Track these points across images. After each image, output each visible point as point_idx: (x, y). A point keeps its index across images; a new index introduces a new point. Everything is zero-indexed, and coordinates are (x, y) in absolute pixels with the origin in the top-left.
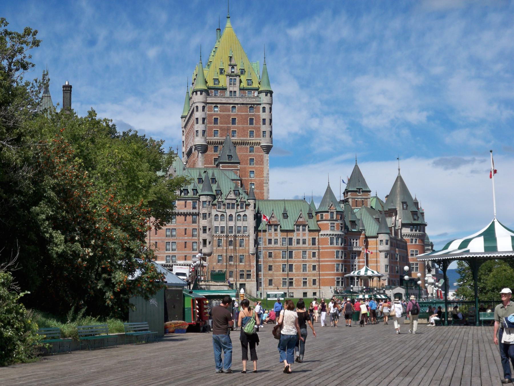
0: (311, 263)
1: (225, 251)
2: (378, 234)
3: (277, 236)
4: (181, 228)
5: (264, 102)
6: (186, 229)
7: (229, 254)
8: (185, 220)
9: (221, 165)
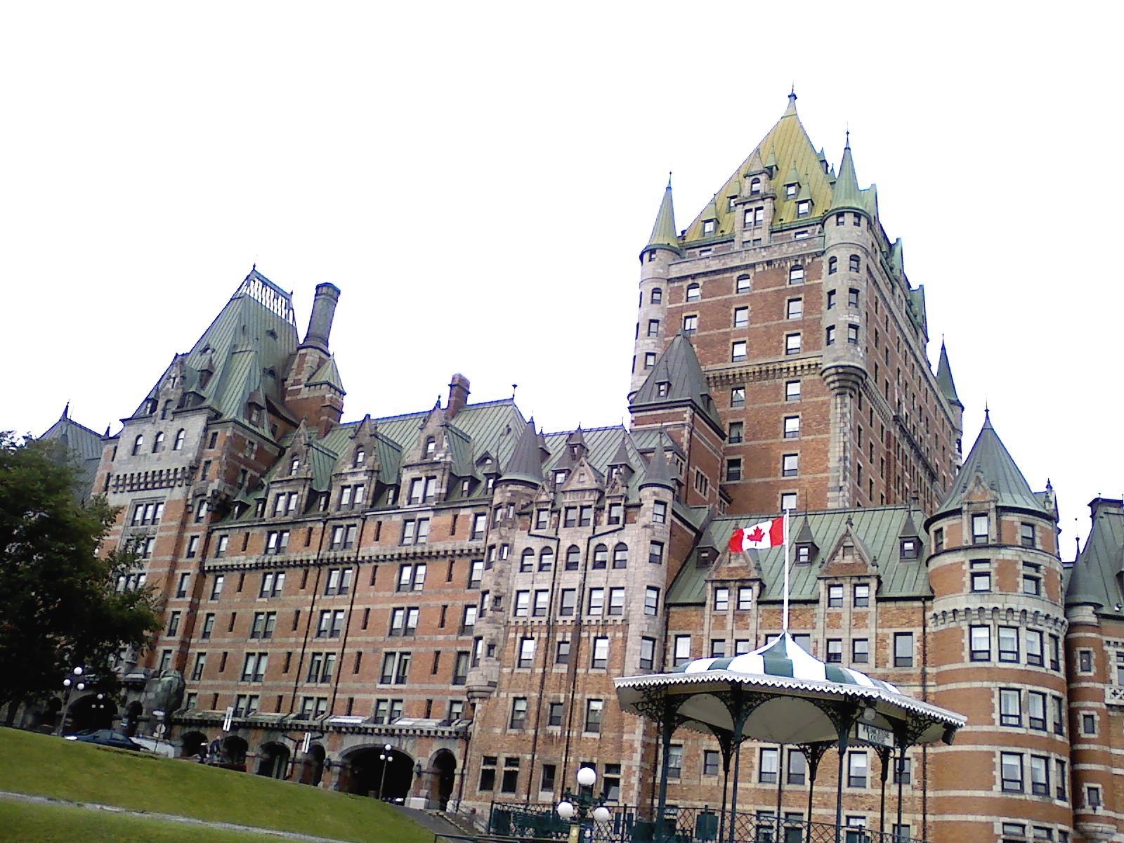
1: (537, 681)
4: (432, 603)
5: (832, 242)
6: (445, 607)
7: (550, 695)
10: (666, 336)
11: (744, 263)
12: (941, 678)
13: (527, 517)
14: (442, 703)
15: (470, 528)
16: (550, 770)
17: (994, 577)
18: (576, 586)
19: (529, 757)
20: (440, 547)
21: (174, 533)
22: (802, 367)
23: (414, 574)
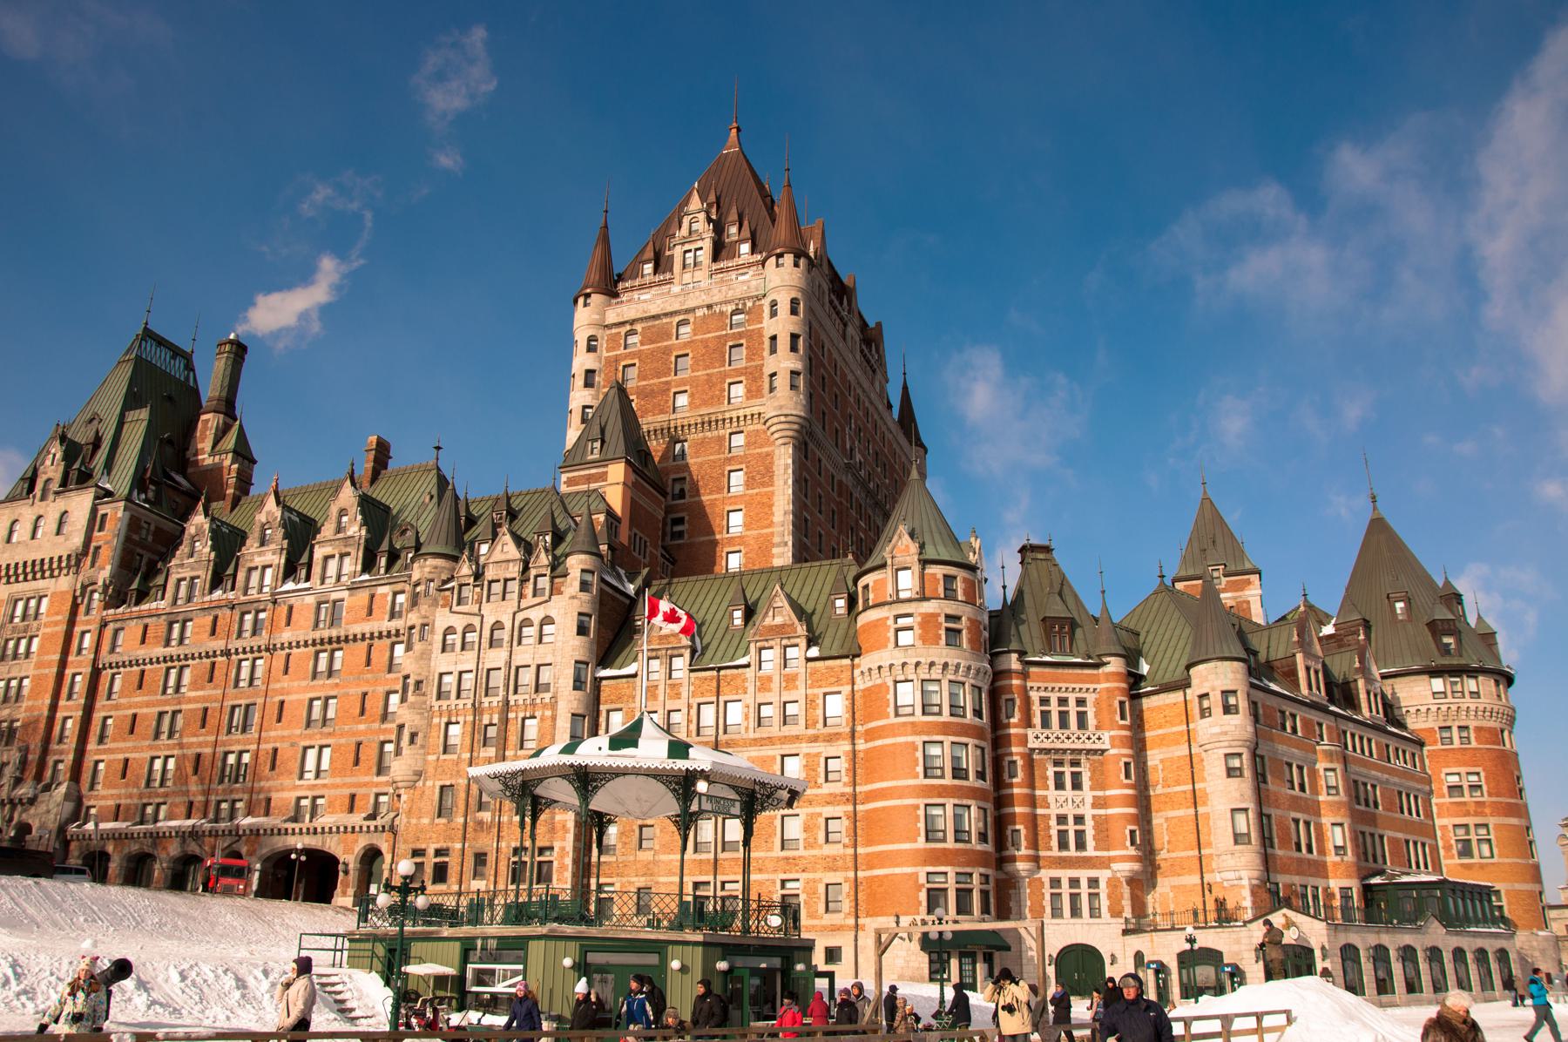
0: (818, 810)
2: (1188, 667)
3: (678, 696)
5: (772, 285)
6: (365, 694)
8: (368, 663)
9: (564, 477)
12: (870, 735)
13: (448, 593)
14: (367, 796)
15: (388, 608)
16: (480, 859)
18: (501, 664)
19: (458, 846)
20: (357, 629)
21: (62, 628)
22: (745, 416)
23: (331, 659)
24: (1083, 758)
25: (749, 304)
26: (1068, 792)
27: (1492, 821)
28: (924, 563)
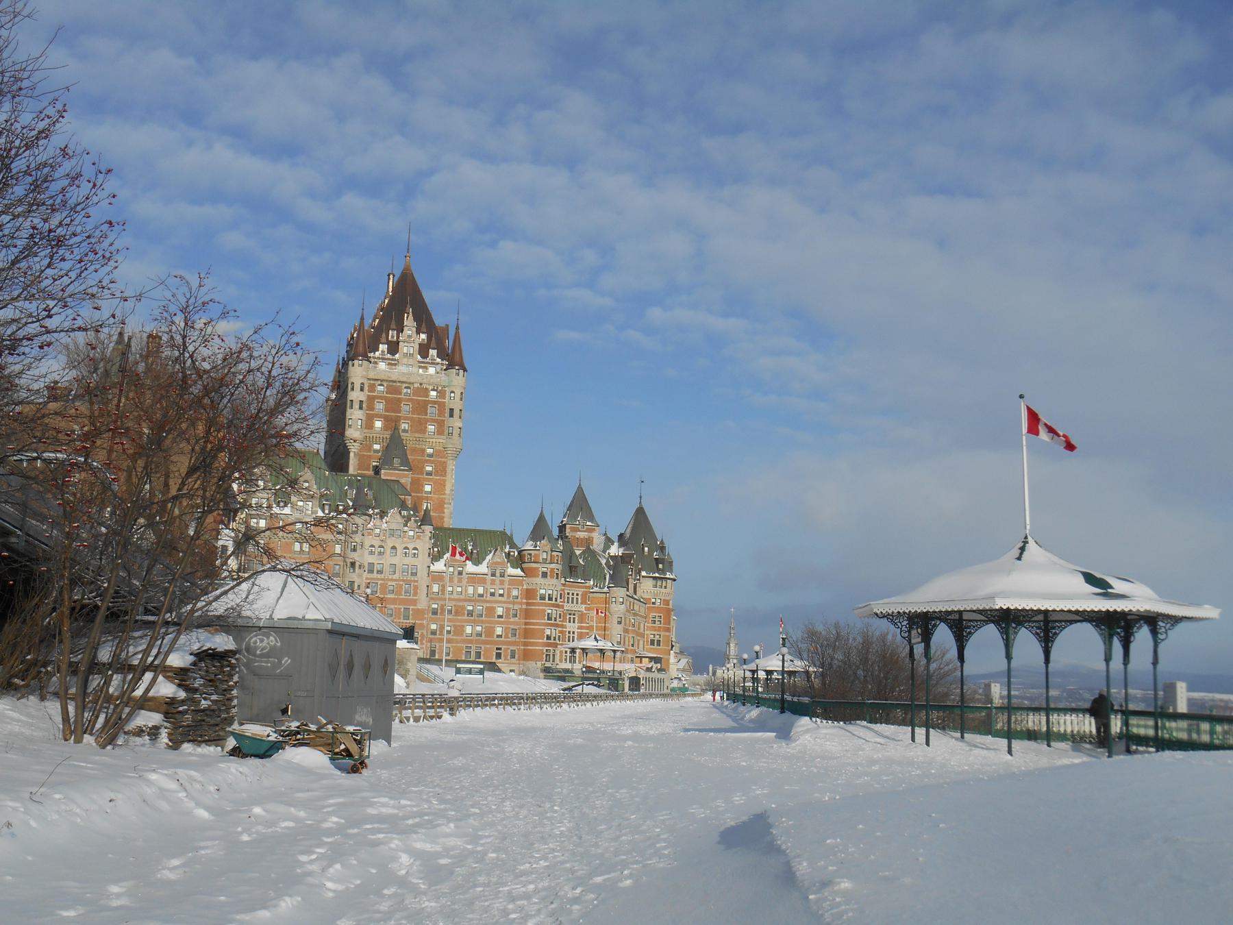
0: (509, 626)
5: (453, 383)
10: (367, 410)
11: (409, 381)
17: (549, 574)
24: (576, 613)
25: (440, 388)
26: (572, 624)
27: (662, 633)
28: (552, 551)
